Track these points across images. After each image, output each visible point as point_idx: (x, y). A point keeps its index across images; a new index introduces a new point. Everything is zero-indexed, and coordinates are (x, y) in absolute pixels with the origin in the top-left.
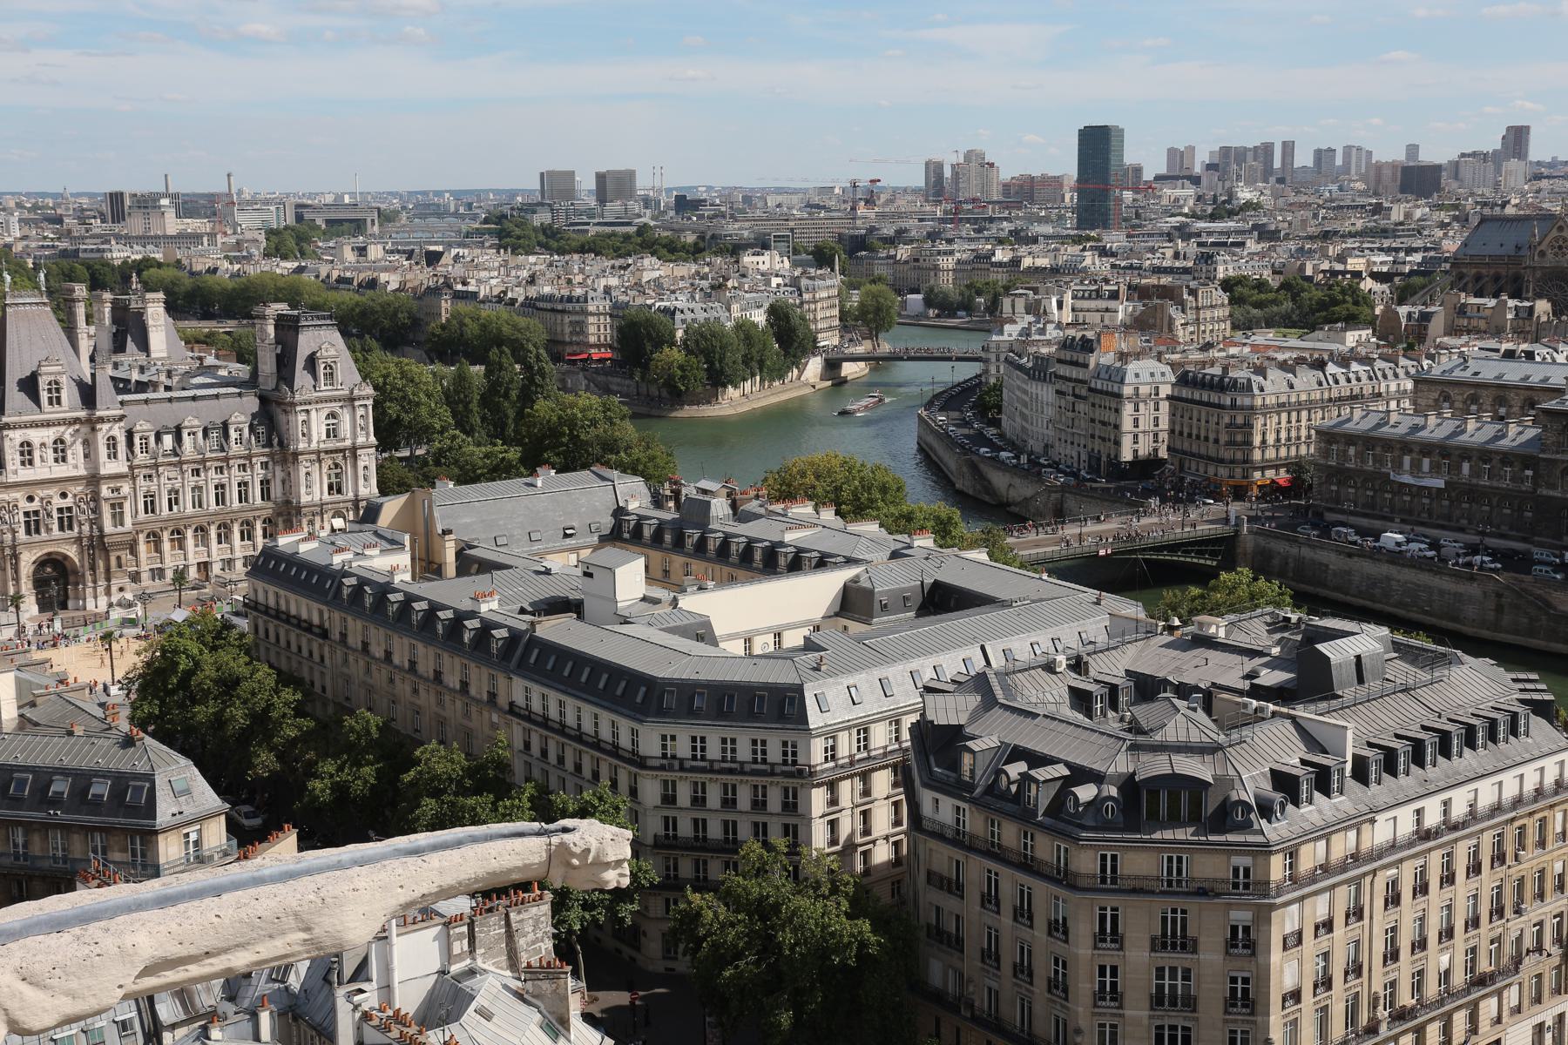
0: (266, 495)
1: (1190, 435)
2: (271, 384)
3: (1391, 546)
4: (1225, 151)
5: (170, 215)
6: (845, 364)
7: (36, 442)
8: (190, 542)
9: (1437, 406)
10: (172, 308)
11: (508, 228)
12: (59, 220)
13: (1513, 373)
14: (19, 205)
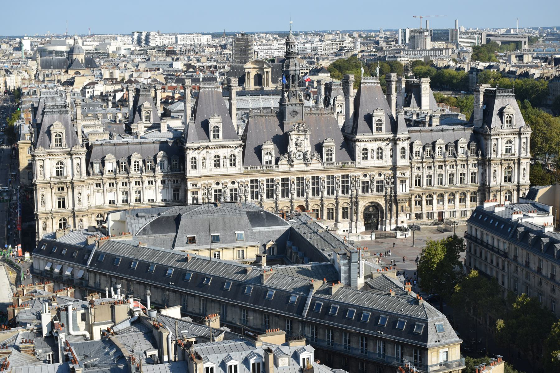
0: (473, 180)
2: (480, 124)
5: (429, 39)
10: (433, 86)
12: (377, 43)
14: (360, 36)
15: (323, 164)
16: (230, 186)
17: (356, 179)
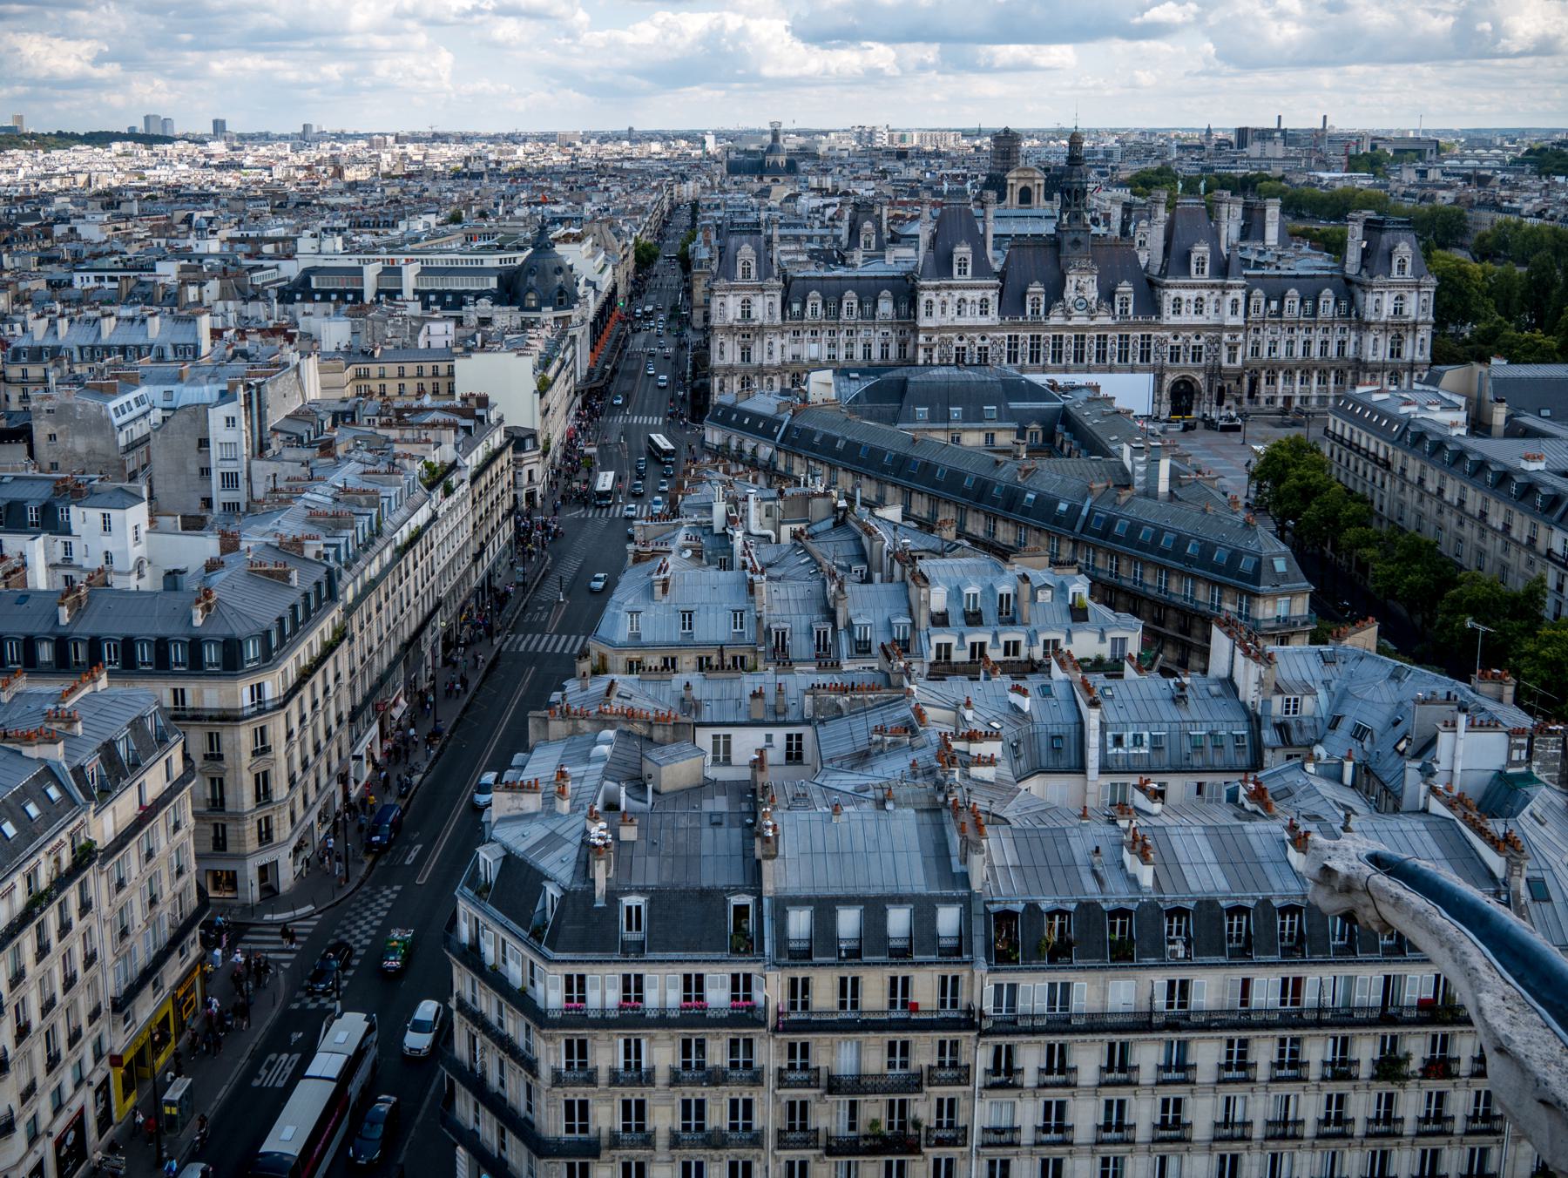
7: (1184, 299)
8: (1280, 380)
15: (1114, 318)
16: (979, 342)
17: (1162, 342)
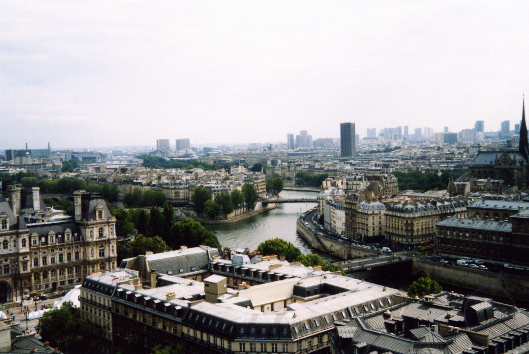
1: (392, 227)
3: (461, 264)
4: (386, 130)
6: (269, 204)
9: (475, 217)
10: (42, 192)
11: (150, 161)
13: (500, 205)
